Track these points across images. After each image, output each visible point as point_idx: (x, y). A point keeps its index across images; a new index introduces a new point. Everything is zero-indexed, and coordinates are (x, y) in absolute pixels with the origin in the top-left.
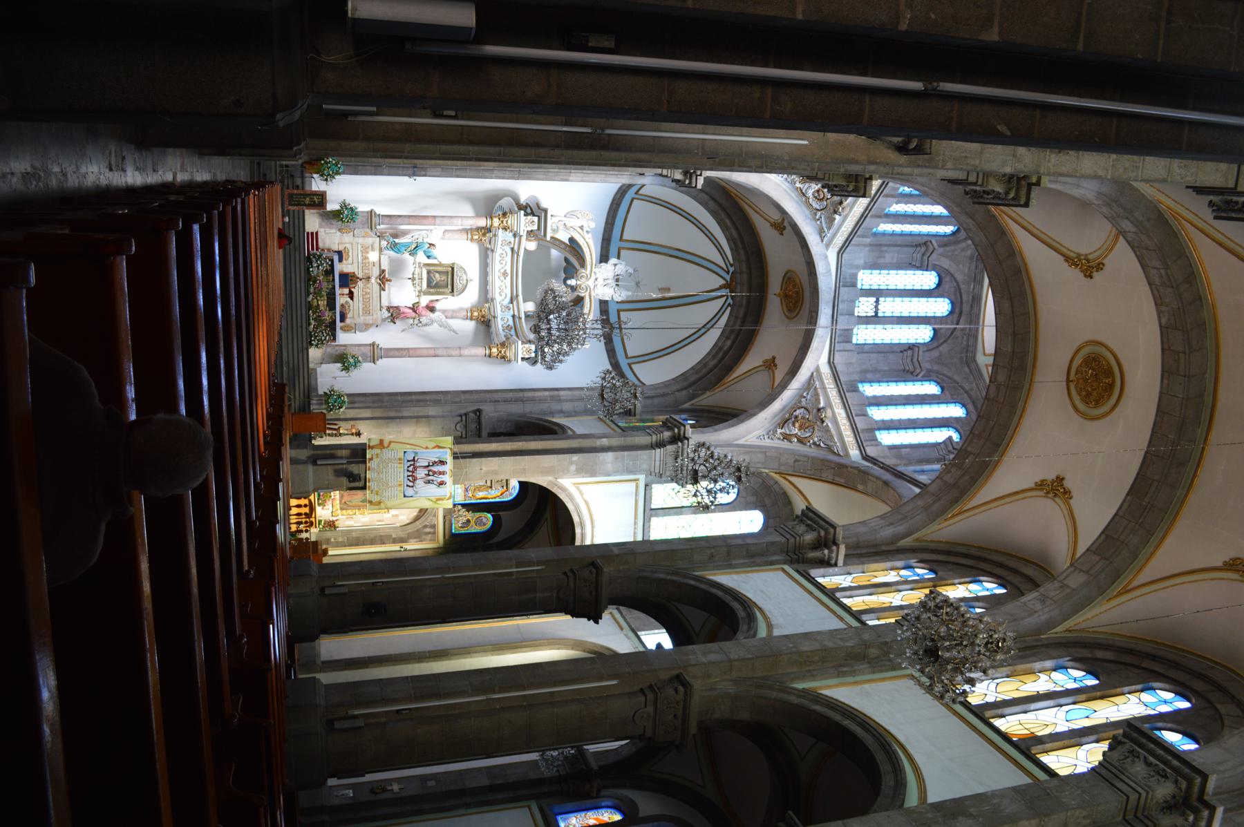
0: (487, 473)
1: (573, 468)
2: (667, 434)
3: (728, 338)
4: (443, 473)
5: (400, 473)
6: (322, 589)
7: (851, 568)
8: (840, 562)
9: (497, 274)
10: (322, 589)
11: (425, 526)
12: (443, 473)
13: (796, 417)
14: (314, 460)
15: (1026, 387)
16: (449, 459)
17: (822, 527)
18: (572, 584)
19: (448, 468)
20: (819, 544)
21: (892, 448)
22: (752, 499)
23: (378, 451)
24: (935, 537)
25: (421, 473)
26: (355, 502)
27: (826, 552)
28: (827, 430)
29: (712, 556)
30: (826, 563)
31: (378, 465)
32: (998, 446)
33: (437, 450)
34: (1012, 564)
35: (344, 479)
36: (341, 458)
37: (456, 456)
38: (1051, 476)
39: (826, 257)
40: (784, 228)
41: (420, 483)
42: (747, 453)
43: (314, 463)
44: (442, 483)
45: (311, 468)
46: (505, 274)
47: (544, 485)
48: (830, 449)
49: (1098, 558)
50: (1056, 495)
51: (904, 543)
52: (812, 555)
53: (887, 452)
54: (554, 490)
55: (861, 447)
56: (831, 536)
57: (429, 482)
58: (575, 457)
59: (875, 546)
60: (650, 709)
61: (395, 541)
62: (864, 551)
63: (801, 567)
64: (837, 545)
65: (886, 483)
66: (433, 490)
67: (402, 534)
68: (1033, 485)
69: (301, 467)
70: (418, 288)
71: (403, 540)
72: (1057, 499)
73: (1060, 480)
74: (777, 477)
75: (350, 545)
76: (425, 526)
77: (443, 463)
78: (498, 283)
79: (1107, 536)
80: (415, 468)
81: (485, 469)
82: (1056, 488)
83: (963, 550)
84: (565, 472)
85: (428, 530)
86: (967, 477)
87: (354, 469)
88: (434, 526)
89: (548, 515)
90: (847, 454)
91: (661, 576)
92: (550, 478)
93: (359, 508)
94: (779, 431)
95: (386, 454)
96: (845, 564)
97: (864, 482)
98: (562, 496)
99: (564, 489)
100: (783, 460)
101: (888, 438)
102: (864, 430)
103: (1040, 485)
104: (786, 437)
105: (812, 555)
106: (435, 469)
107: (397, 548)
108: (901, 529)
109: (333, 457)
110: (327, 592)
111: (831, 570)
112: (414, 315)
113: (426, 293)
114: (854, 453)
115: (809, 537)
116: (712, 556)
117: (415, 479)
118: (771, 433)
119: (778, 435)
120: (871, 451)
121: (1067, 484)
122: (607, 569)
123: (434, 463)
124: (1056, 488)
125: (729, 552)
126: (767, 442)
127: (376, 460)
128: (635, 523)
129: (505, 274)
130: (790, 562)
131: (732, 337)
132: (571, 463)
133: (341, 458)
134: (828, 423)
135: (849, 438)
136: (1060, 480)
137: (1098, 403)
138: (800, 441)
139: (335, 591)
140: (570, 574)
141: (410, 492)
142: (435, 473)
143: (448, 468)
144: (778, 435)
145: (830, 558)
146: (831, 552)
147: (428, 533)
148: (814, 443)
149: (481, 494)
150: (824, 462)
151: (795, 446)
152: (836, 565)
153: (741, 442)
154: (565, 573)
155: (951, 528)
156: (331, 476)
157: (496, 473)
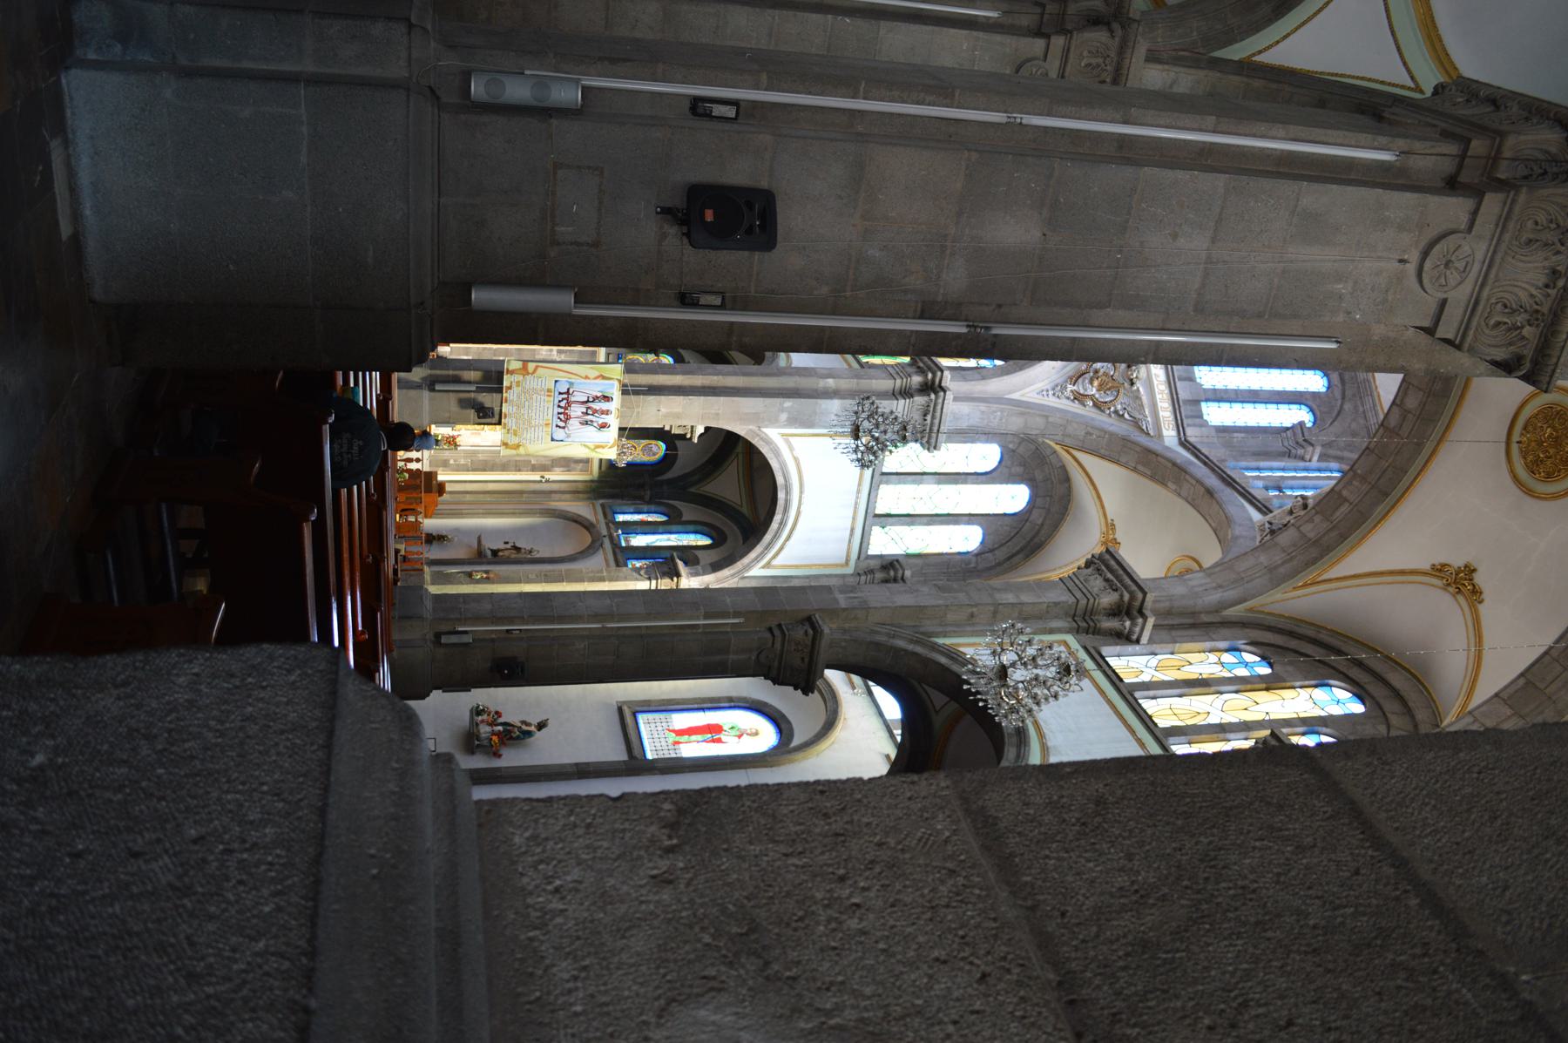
0: (666, 416)
1: (784, 416)
2: (917, 379)
4: (607, 412)
5: (547, 409)
6: (438, 636)
7: (1155, 647)
8: (1144, 639)
10: (438, 636)
12: (607, 412)
13: (1096, 372)
14: (431, 384)
15: (1445, 419)
16: (616, 393)
17: (1126, 588)
18: (778, 645)
19: (614, 406)
20: (1117, 611)
21: (1223, 430)
22: (1019, 470)
24: (1277, 609)
25: (576, 411)
27: (1128, 624)
28: (1137, 397)
29: (972, 615)
30: (1125, 638)
31: (519, 397)
32: (1387, 495)
33: (600, 381)
34: (1378, 666)
35: (472, 413)
36: (469, 382)
37: (626, 391)
38: (1457, 561)
41: (574, 423)
42: (1022, 414)
43: (432, 390)
44: (604, 426)
45: (426, 394)
47: (742, 433)
48: (1136, 423)
49: (1509, 712)
50: (1459, 591)
51: (1232, 612)
52: (1109, 624)
53: (1213, 433)
54: (755, 442)
55: (1180, 427)
56: (1137, 604)
57: (586, 423)
58: (788, 403)
59: (1193, 614)
61: (534, 469)
62: (1176, 621)
63: (1090, 640)
64: (1145, 618)
65: (1210, 492)
66: (591, 434)
68: (1426, 566)
69: (412, 393)
72: (1460, 598)
73: (1470, 570)
74: (1058, 448)
77: (607, 398)
79: (1528, 683)
80: (569, 404)
81: (663, 410)
82: (1461, 582)
83: (1310, 632)
84: (773, 422)
86: (1334, 534)
87: (487, 399)
90: (1160, 435)
91: (901, 643)
94: (1070, 387)
95: (530, 382)
96: (1151, 641)
97: (1178, 481)
98: (764, 450)
99: (768, 442)
100: (1070, 430)
101: (1217, 414)
102: (1187, 402)
103: (1439, 570)
104: (1079, 398)
105: (1109, 624)
106: (596, 406)
107: (537, 478)
108: (1230, 594)
109: (457, 380)
110: (444, 640)
111: (1130, 648)
114: (1169, 434)
115: (1108, 599)
116: (972, 615)
117: (568, 418)
118: (1058, 389)
119: (1068, 393)
120: (1192, 434)
121: (1478, 579)
122: (828, 628)
123: (596, 399)
124: (1461, 582)
125: (995, 613)
126: (1052, 401)
127: (515, 389)
128: (858, 491)
130: (1077, 631)
132: (782, 410)
133: (469, 382)
134: (1139, 385)
135: (1166, 413)
136: (1470, 570)
137: (1549, 476)
138: (1096, 405)
139: (454, 639)
140: (777, 632)
141: (559, 434)
142: (595, 411)
143: (614, 406)
144: (1068, 393)
145: (1131, 632)
146: (1134, 624)
148: (1116, 412)
150: (1126, 442)
151: (1088, 411)
152: (1138, 641)
153: (1015, 396)
154: (770, 630)
155: (1297, 600)
156: (454, 407)
157: (678, 416)
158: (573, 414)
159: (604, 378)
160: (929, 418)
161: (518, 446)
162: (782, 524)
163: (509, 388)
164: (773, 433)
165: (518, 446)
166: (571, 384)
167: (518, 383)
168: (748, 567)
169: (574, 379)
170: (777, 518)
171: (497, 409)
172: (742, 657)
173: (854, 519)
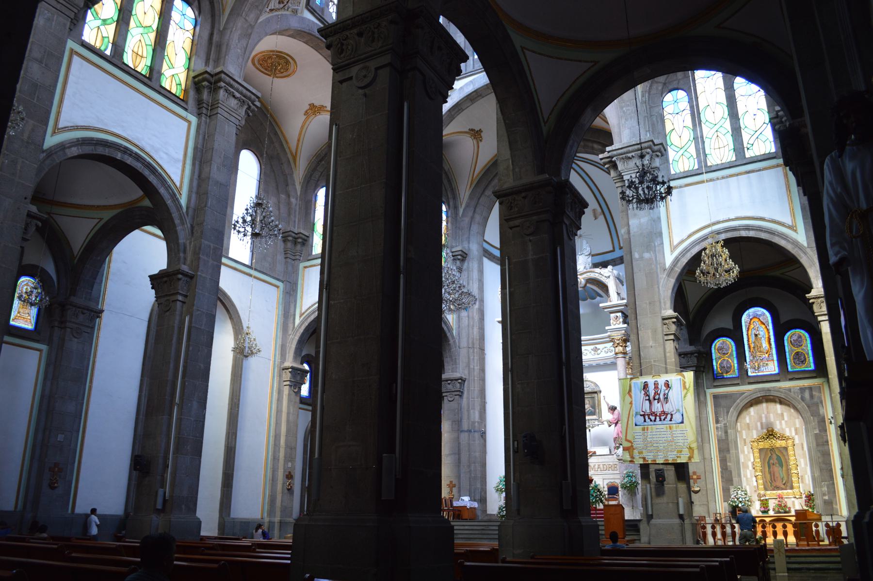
0: (655, 340)
1: (647, 255)
3: (593, 148)
4: (656, 385)
5: (659, 429)
9: (596, 356)
11: (803, 399)
12: (656, 385)
16: (642, 380)
19: (651, 380)
23: (636, 452)
25: (657, 407)
26: (783, 474)
31: (651, 451)
33: (633, 394)
39: (461, 88)
40: (472, 130)
41: (668, 408)
44: (667, 385)
45: (653, 521)
46: (596, 350)
47: (672, 281)
54: (678, 269)
57: (666, 399)
60: (354, 71)
61: (824, 429)
67: (814, 422)
70: (596, 423)
71: (822, 422)
75: (831, 477)
76: (803, 399)
77: (646, 386)
78: (603, 355)
80: (653, 413)
85: (807, 395)
88: (802, 390)
89: (777, 273)
92: (663, 276)
93: (788, 470)
95: (638, 443)
99: (676, 261)
112: (619, 425)
113: (600, 416)
117: (664, 413)
127: (645, 454)
129: (596, 350)
131: (590, 144)
132: (641, 258)
141: (677, 417)
143: (651, 380)
147: (812, 396)
149: (765, 345)
157: (655, 331)
158: (660, 409)
159: (630, 391)
160: (630, 155)
161: (690, 448)
162: (747, 228)
163: (644, 459)
164: (669, 259)
165: (690, 448)
166: (637, 414)
167: (640, 453)
168: (796, 243)
169: (633, 413)
170: (744, 234)
171: (661, 467)
172: (530, 246)
173: (737, 175)
